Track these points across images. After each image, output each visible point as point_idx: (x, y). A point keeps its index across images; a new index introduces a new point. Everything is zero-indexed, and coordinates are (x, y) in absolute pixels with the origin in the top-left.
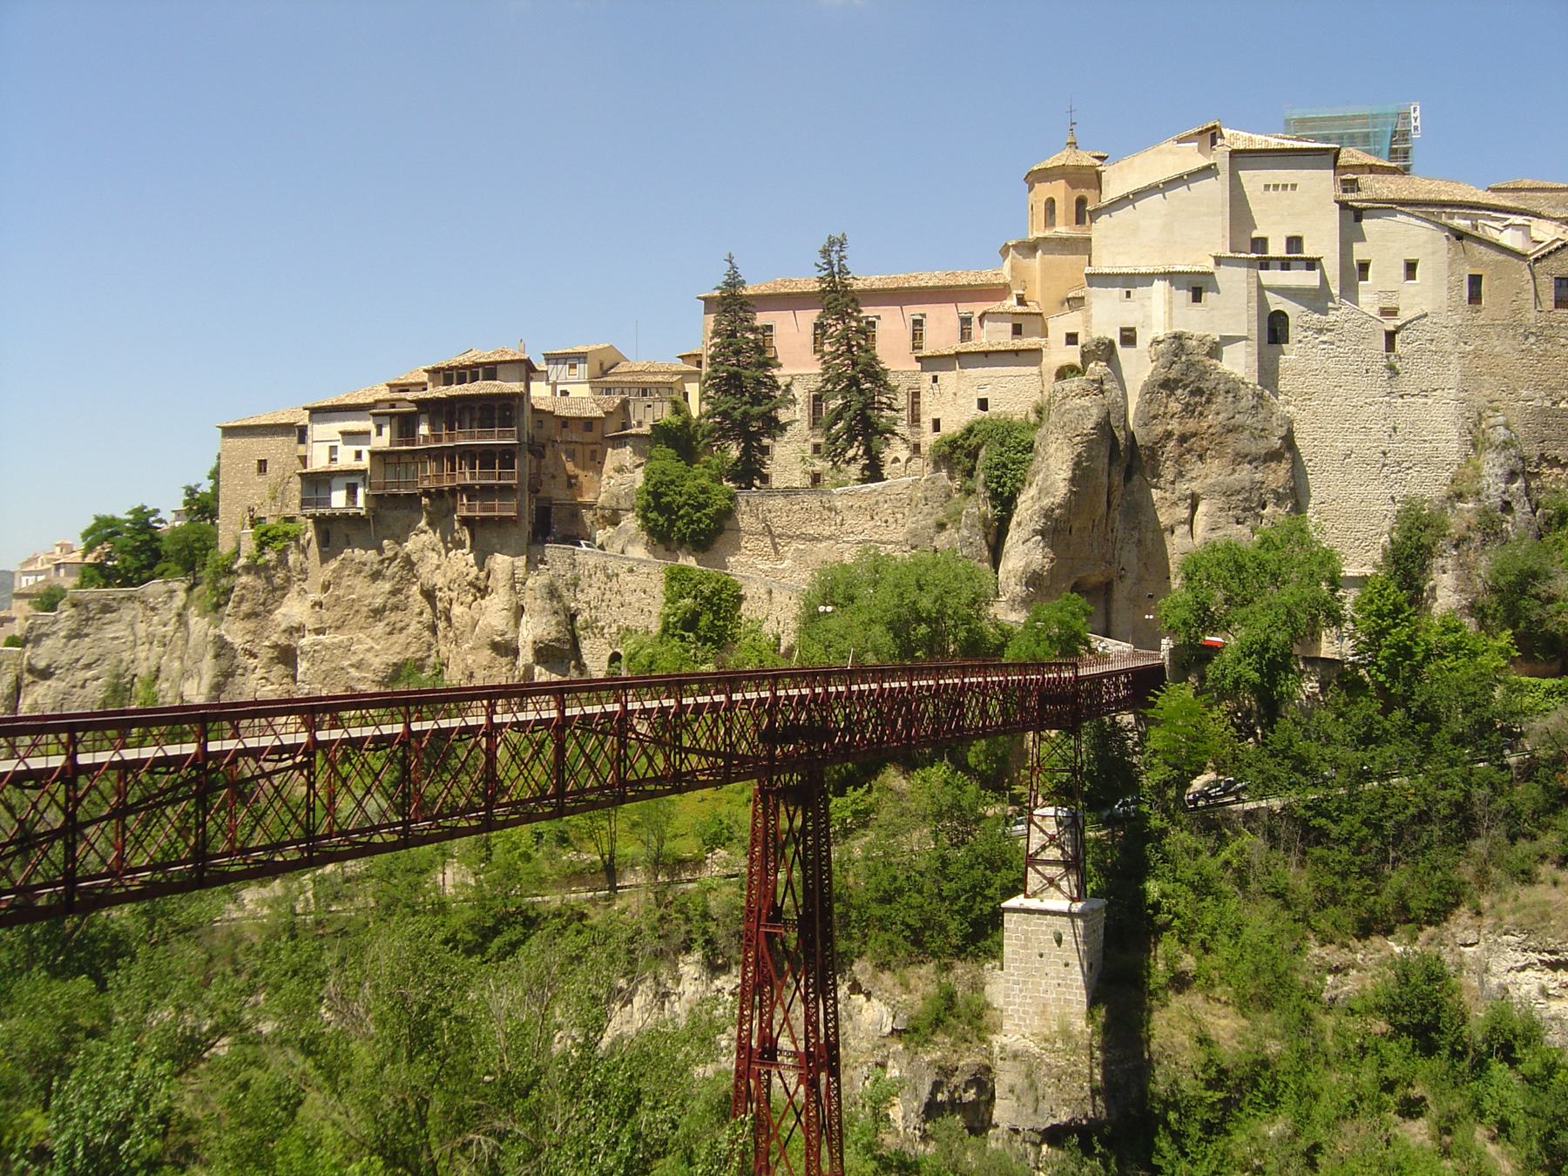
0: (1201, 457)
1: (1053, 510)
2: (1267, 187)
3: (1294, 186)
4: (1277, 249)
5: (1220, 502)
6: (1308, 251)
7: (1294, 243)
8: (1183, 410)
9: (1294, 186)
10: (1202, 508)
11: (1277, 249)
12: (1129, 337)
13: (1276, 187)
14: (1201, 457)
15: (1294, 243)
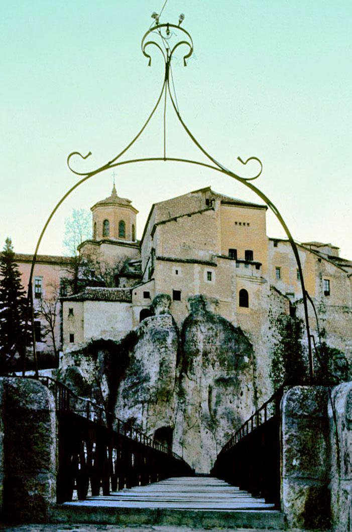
0: (213, 365)
1: (149, 390)
2: (236, 223)
3: (248, 224)
4: (241, 256)
5: (222, 389)
6: (255, 260)
7: (249, 254)
8: (204, 339)
9: (248, 224)
10: (214, 393)
11: (241, 256)
12: (177, 295)
13: (240, 224)
14: (213, 365)
15: (249, 254)
